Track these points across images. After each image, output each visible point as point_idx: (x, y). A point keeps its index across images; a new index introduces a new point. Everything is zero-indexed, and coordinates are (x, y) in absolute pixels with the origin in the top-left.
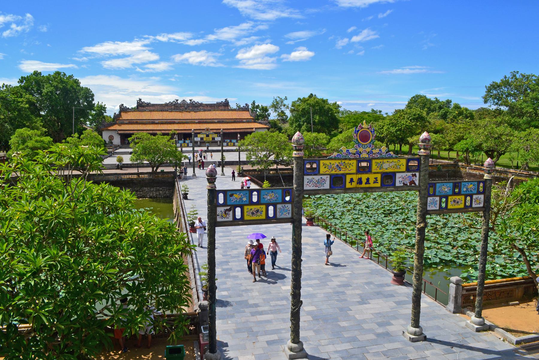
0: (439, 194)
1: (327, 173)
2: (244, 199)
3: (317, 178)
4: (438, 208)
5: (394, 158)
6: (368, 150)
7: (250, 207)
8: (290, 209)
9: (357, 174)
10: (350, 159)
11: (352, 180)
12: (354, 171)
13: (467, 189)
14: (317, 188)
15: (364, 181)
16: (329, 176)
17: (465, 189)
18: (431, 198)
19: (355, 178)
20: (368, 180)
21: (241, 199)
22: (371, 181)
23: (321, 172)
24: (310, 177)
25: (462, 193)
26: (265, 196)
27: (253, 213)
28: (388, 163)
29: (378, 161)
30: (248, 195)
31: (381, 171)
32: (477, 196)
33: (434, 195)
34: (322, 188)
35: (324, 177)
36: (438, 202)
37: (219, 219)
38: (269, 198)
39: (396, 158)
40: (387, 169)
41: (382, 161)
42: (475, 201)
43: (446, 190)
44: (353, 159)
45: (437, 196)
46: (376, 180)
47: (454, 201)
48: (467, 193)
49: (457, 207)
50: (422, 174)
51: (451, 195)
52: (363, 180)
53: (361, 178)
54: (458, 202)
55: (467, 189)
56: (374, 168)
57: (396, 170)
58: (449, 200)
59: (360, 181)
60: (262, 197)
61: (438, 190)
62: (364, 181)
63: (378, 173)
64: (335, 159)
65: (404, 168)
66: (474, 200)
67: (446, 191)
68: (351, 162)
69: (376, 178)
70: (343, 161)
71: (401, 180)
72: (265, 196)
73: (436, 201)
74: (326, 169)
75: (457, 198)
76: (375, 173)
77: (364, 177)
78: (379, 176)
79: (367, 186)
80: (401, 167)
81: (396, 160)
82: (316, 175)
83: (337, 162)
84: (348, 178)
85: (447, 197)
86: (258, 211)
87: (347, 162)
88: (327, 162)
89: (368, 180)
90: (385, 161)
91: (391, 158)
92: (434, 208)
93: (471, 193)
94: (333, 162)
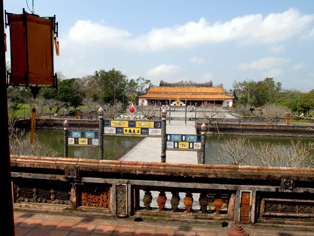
0: (174, 140)
1: (114, 126)
2: (79, 135)
3: (110, 128)
4: (173, 147)
5: (147, 121)
6: (134, 116)
7: (81, 139)
8: (98, 141)
9: (128, 127)
10: (125, 120)
11: (126, 130)
12: (128, 126)
13: (190, 139)
14: (110, 133)
15: (132, 131)
16: (115, 128)
17: (189, 139)
18: (169, 142)
19: (128, 129)
20: (134, 131)
21: (78, 135)
22: (136, 131)
23: (112, 126)
24: (107, 128)
25: (187, 141)
26: (87, 135)
27: (82, 142)
28: (144, 123)
29: (139, 122)
30: (80, 133)
31: (140, 127)
32: (197, 143)
33: (170, 140)
34: (112, 133)
35: (113, 128)
36: (173, 145)
37: (69, 143)
38: (89, 135)
39: (148, 121)
40: (143, 126)
41: (141, 122)
42: (196, 146)
43: (177, 138)
44: (126, 121)
45: (172, 141)
46: (138, 131)
47: (182, 145)
48: (190, 141)
49: (184, 148)
50: (162, 129)
51: (180, 142)
52: (131, 131)
53: (131, 130)
54: (184, 145)
55: (190, 139)
56: (137, 125)
57: (149, 127)
58: (179, 144)
59: (130, 131)
60: (86, 135)
61: (172, 138)
62: (132, 131)
63: (139, 128)
64: (118, 120)
65: (153, 126)
66: (194, 145)
67: (177, 139)
68: (125, 122)
69: (138, 130)
70: (122, 121)
71: (151, 132)
72: (87, 135)
73: (172, 144)
74: (114, 125)
75: (184, 143)
76: (137, 128)
77: (132, 129)
78: (140, 129)
79: (134, 133)
80: (151, 125)
81: (148, 122)
82: (109, 127)
83: (119, 122)
84: (124, 129)
85: (178, 142)
86: (84, 141)
87: (123, 122)
88: (114, 121)
89: (134, 131)
90: (142, 122)
91: (145, 121)
92: (171, 147)
93: (193, 141)
94: (117, 121)
